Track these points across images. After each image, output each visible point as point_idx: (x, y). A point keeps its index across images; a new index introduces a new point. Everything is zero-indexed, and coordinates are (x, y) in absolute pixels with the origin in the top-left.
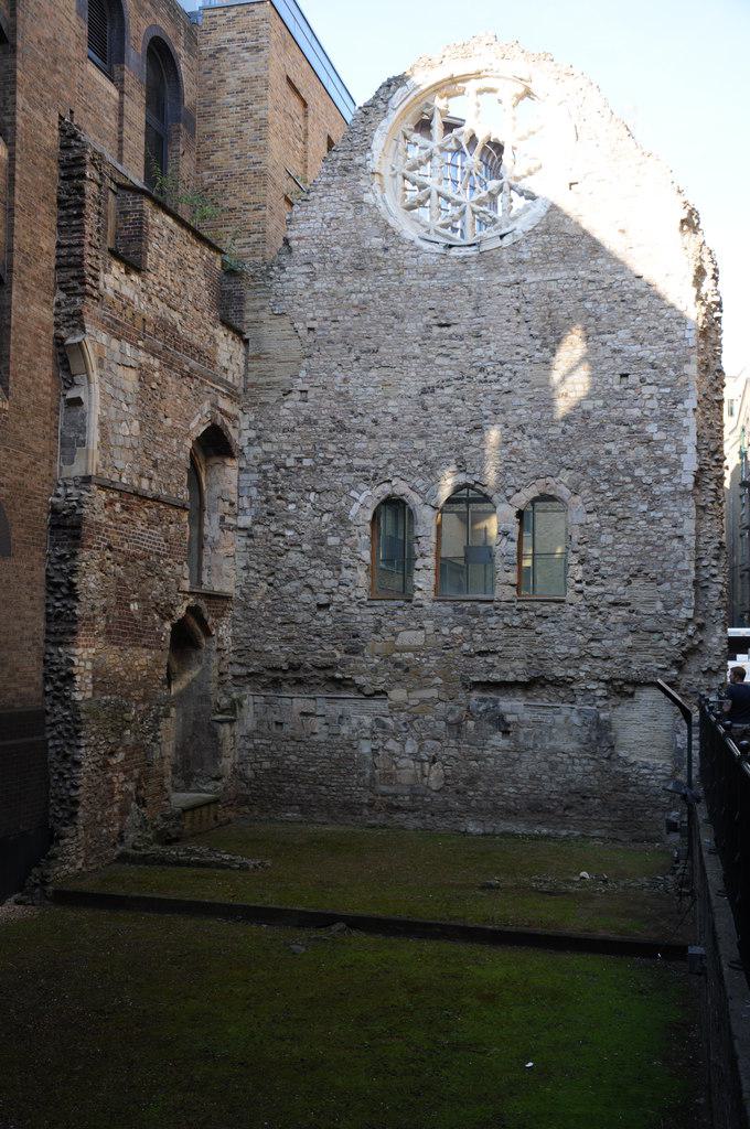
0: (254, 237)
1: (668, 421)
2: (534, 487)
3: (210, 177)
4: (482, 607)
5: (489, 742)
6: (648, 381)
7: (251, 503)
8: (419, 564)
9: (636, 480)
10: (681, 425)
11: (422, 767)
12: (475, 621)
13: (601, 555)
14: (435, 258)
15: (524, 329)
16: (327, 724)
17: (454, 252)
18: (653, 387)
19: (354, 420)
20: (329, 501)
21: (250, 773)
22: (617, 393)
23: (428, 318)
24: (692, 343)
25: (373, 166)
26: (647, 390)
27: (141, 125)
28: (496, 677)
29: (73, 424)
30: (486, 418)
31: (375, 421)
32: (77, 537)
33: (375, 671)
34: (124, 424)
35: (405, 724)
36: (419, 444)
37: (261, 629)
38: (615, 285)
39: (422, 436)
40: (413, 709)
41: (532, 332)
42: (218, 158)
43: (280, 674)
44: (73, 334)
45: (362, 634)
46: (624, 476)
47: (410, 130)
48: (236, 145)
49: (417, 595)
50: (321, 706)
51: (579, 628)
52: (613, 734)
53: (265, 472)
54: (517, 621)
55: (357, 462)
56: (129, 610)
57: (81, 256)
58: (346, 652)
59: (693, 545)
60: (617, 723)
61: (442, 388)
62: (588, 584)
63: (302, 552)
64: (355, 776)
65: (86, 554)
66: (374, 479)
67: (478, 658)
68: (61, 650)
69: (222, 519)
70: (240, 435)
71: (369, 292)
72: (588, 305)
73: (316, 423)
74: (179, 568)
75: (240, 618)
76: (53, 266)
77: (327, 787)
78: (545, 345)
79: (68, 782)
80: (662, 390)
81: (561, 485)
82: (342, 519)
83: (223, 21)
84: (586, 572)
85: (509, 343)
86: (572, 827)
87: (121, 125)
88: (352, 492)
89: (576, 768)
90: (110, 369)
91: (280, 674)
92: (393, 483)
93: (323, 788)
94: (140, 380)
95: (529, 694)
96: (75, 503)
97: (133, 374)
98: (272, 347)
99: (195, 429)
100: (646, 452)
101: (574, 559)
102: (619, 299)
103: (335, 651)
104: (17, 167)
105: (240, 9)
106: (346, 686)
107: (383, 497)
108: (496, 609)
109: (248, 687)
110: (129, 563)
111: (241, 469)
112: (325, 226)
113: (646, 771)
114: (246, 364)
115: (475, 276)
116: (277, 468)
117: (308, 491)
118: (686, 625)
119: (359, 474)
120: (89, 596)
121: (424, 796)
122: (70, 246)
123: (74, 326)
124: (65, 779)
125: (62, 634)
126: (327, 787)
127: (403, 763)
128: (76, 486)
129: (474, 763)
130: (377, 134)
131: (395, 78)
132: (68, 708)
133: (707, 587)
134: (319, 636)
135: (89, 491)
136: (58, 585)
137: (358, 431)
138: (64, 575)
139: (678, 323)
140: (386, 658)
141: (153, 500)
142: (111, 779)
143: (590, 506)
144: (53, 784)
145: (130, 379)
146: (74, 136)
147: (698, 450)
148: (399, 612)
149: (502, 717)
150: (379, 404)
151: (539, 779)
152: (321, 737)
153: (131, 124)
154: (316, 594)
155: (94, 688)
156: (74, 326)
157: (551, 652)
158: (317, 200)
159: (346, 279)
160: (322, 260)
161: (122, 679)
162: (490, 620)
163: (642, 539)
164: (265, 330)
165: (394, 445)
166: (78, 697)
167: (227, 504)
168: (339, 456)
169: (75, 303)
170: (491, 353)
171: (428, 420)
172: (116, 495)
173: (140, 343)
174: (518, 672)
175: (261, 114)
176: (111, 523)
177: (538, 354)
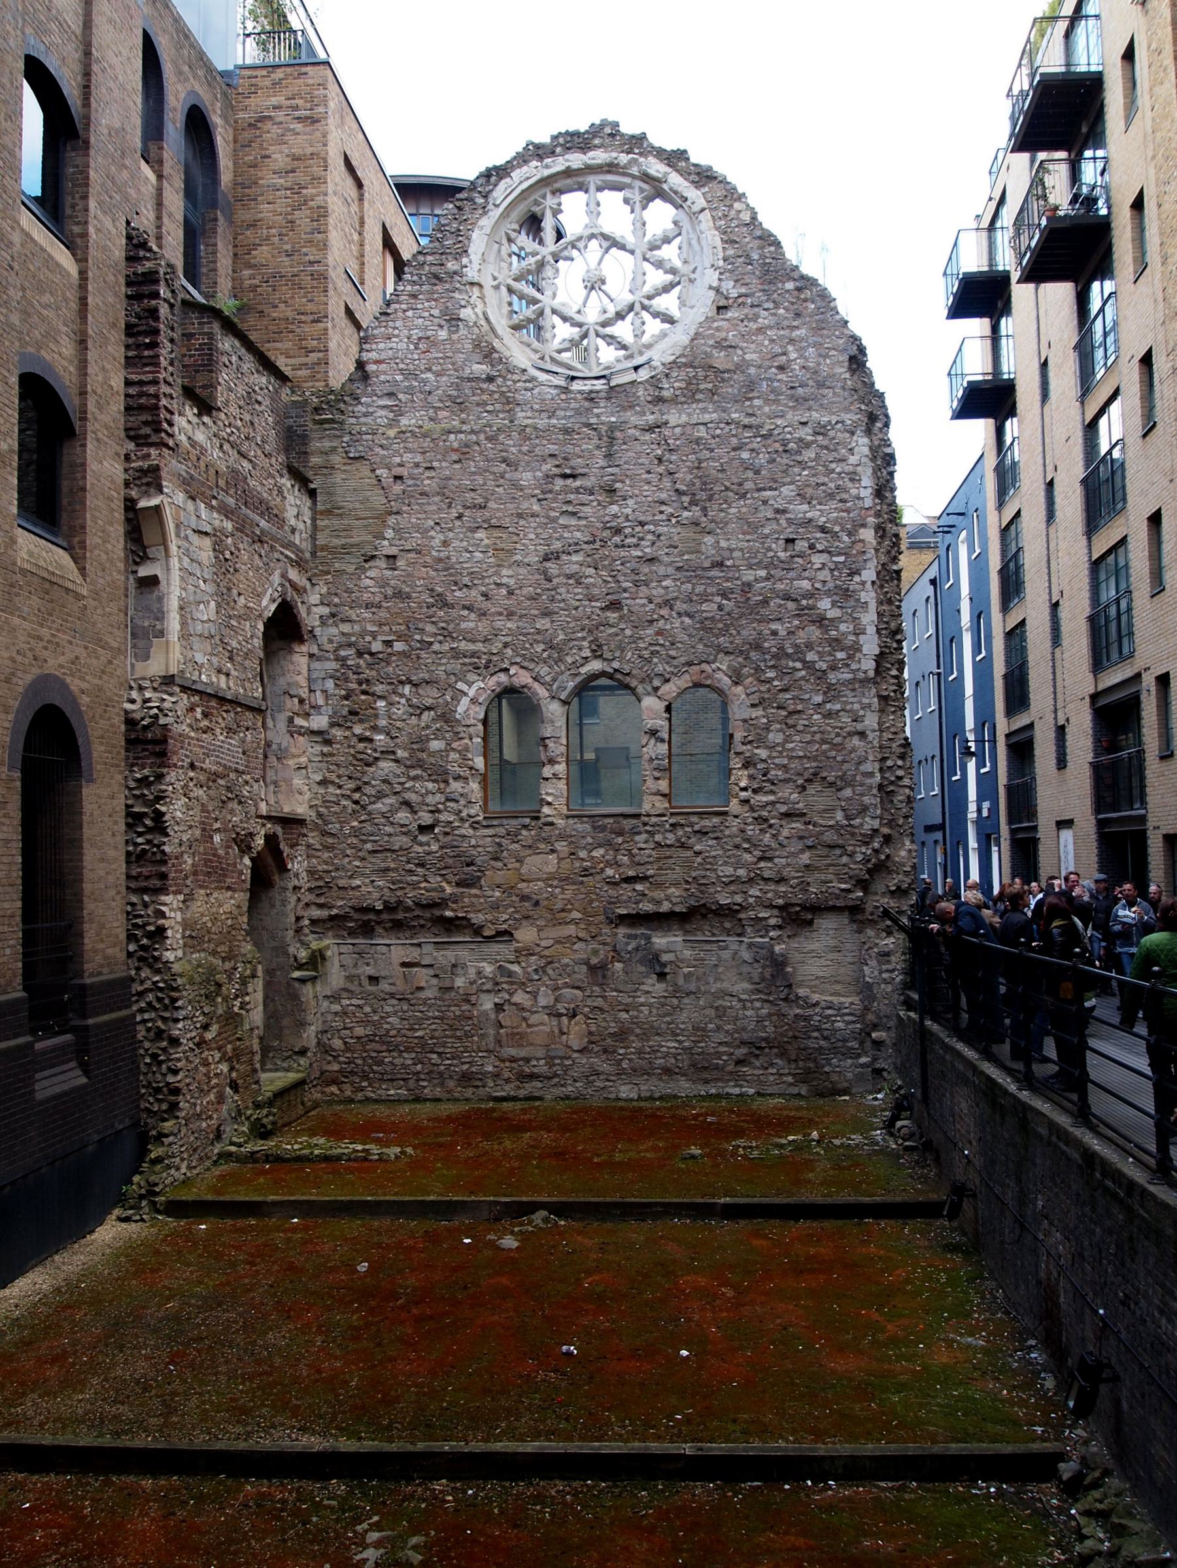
0: (314, 357)
1: (844, 595)
2: (687, 676)
3: (252, 277)
4: (627, 824)
5: (641, 987)
6: (819, 547)
7: (327, 698)
8: (547, 771)
9: (808, 666)
10: (858, 600)
11: (559, 1023)
12: (620, 840)
13: (769, 757)
14: (554, 392)
15: (667, 483)
16: (436, 976)
17: (576, 386)
18: (825, 555)
19: (458, 594)
20: (429, 695)
21: (337, 1043)
22: (782, 562)
23: (549, 466)
24: (868, 503)
25: (471, 274)
26: (818, 560)
27: (181, 219)
28: (647, 907)
29: (148, 609)
30: (625, 590)
31: (485, 595)
32: (163, 754)
33: (495, 907)
34: (202, 606)
35: (536, 970)
36: (543, 623)
37: (347, 860)
38: (776, 432)
39: (546, 614)
40: (546, 953)
41: (677, 486)
42: (262, 254)
43: (372, 916)
44: (147, 494)
45: (478, 861)
46: (794, 661)
47: (514, 230)
48: (286, 238)
49: (546, 810)
50: (429, 954)
51: (746, 846)
52: (789, 969)
53: (344, 659)
54: (671, 838)
55: (464, 646)
56: (212, 843)
57: (156, 396)
58: (458, 885)
59: (876, 743)
60: (795, 957)
61: (569, 554)
62: (755, 791)
63: (397, 761)
64: (476, 1038)
66: (486, 667)
67: (625, 885)
68: (146, 898)
69: (291, 720)
70: (311, 612)
71: (473, 432)
72: (745, 455)
73: (409, 597)
74: (256, 786)
75: (318, 847)
76: (122, 408)
77: (439, 1054)
78: (693, 503)
79: (164, 1066)
80: (835, 559)
81: (720, 671)
82: (447, 717)
83: (267, 82)
84: (751, 777)
85: (649, 499)
86: (745, 1084)
87: (159, 218)
88: (459, 683)
89: (748, 1013)
90: (186, 538)
91: (372, 916)
92: (512, 672)
93: (435, 1056)
94: (214, 550)
95: (688, 927)
96: (156, 711)
97: (207, 542)
98: (347, 500)
99: (266, 607)
100: (818, 633)
101: (736, 763)
102: (781, 449)
103: (444, 884)
104: (90, 288)
105: (288, 70)
106: (457, 927)
107: (498, 690)
108: (645, 824)
109: (330, 933)
110: (211, 784)
111: (311, 656)
112: (412, 347)
113: (829, 1012)
114: (314, 520)
115: (605, 415)
116: (360, 654)
117: (402, 683)
118: (872, 837)
119: (467, 660)
120: (176, 828)
121: (561, 1058)
122: (141, 383)
123: (148, 484)
124: (162, 1062)
125: (147, 878)
126: (439, 1054)
127: (534, 1019)
128: (155, 689)
129: (624, 1015)
130: (475, 235)
131: (496, 168)
132: (158, 972)
133: (892, 791)
134: (422, 865)
135: (171, 695)
136: (139, 817)
137: (465, 607)
138: (147, 803)
139: (852, 480)
140: (508, 890)
141: (230, 701)
142: (207, 1059)
143: (755, 699)
144: (143, 1069)
145: (204, 550)
146: (144, 245)
147: (878, 631)
148: (524, 832)
149: (656, 957)
150: (490, 573)
151: (704, 1030)
152: (428, 994)
153: (170, 215)
154: (416, 812)
156: (148, 484)
157: (713, 875)
158: (400, 314)
159: (442, 414)
160: (410, 391)
162: (637, 838)
163: (818, 737)
164: (338, 477)
165: (509, 625)
166: (169, 956)
167: (296, 700)
168: (441, 638)
169: (149, 455)
170: (629, 511)
171: (553, 593)
172: (197, 698)
173: (214, 502)
174: (674, 900)
175: (319, 200)
176: (192, 734)
177: (686, 514)
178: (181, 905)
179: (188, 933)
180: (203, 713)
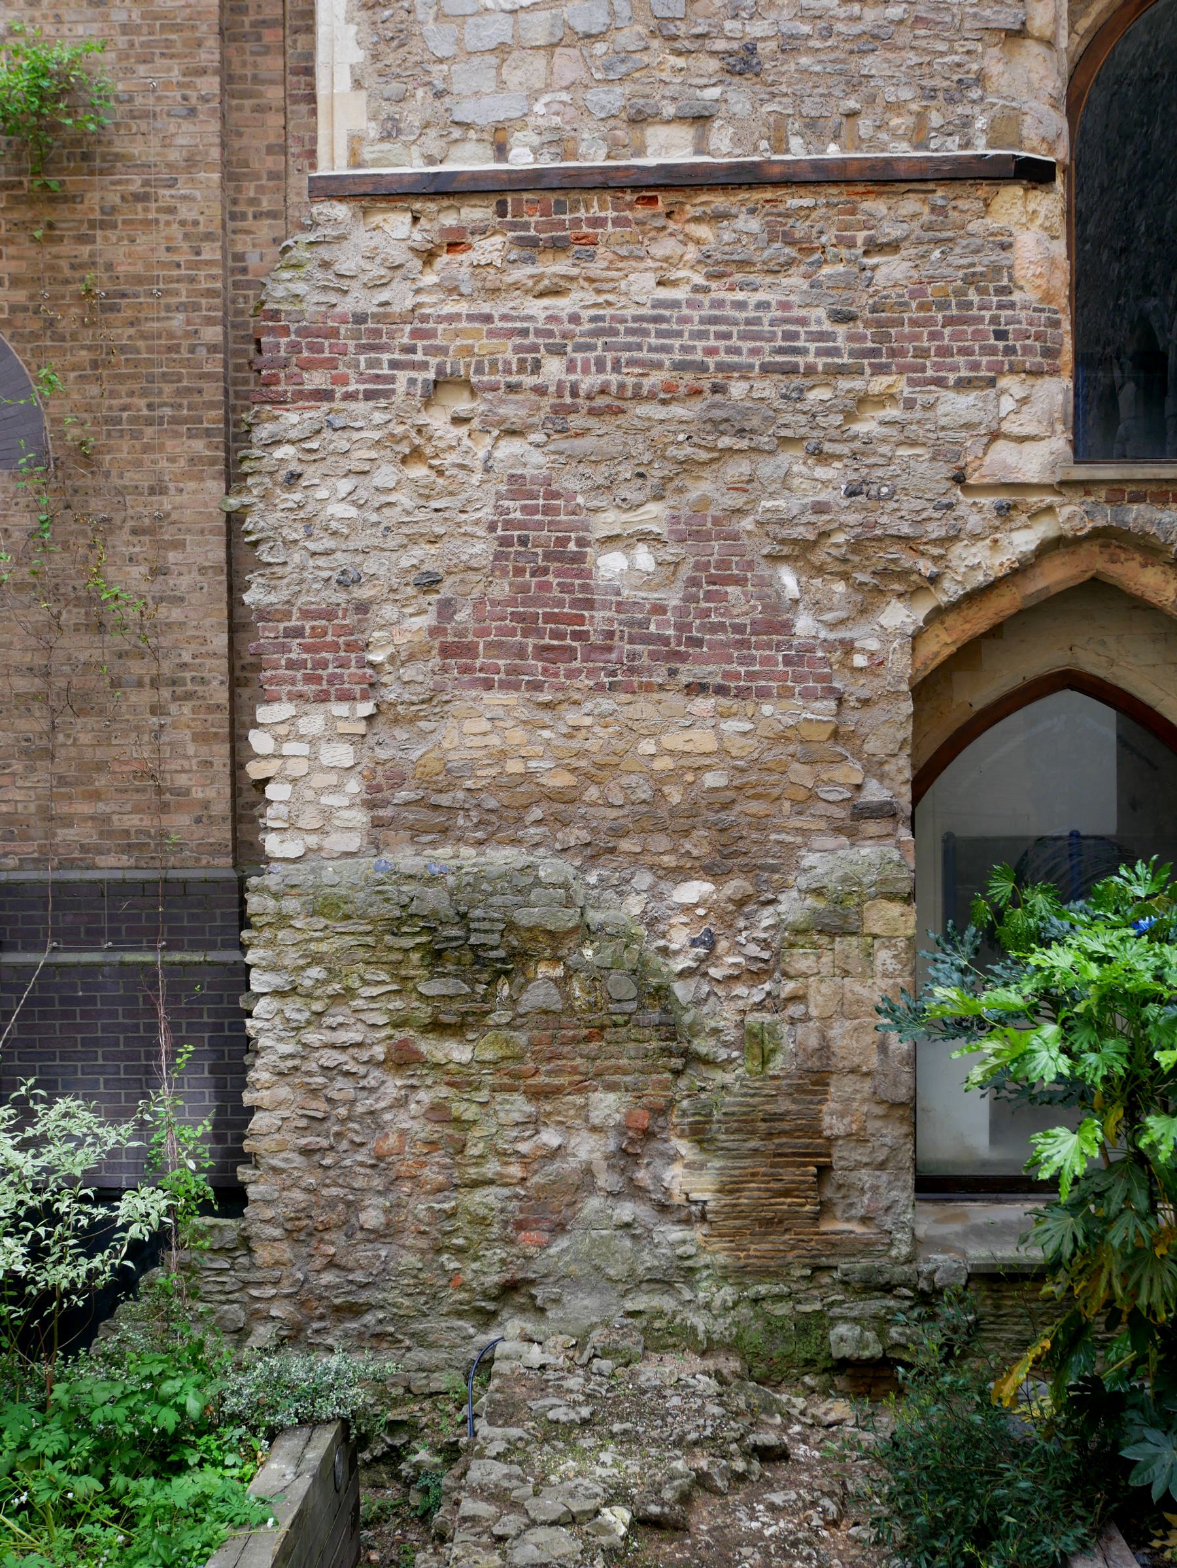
65: (292, 419)
155: (377, 823)
161: (566, 797)
172: (476, 213)
176: (463, 308)
178: (361, 728)
179: (402, 795)
180: (521, 242)
